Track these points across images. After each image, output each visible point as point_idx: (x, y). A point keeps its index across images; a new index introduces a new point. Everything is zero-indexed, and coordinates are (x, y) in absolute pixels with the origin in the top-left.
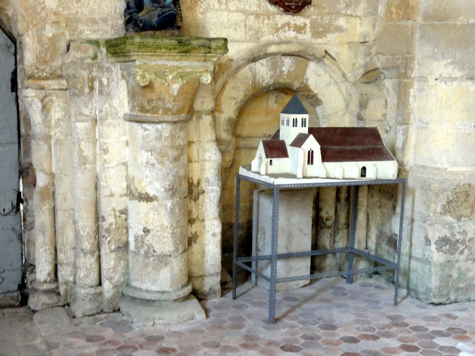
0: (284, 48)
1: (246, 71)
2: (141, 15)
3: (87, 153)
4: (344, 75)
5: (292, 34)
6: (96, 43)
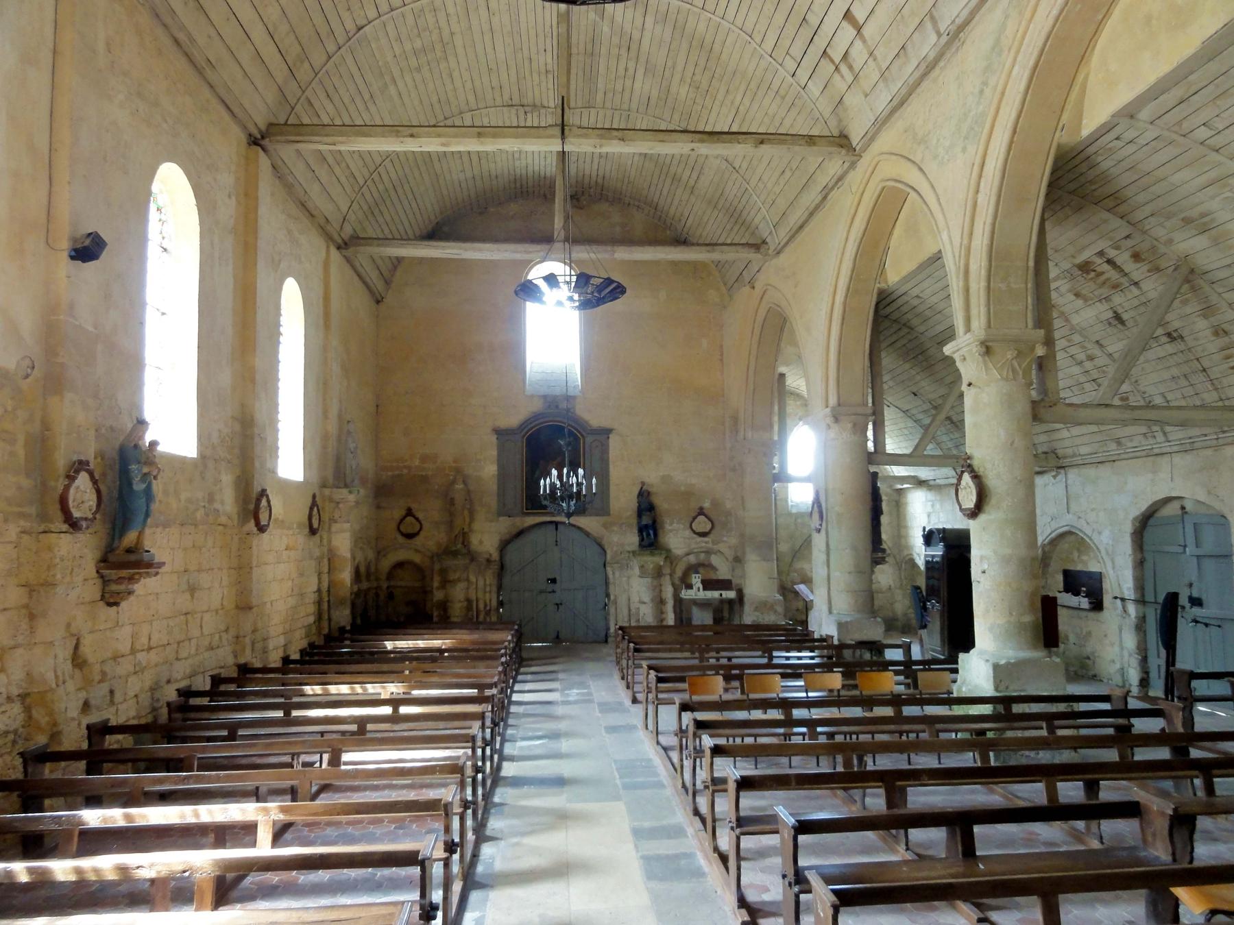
0: (699, 550)
1: (685, 559)
2: (643, 543)
3: (626, 587)
4: (727, 559)
5: (704, 544)
6: (629, 552)
